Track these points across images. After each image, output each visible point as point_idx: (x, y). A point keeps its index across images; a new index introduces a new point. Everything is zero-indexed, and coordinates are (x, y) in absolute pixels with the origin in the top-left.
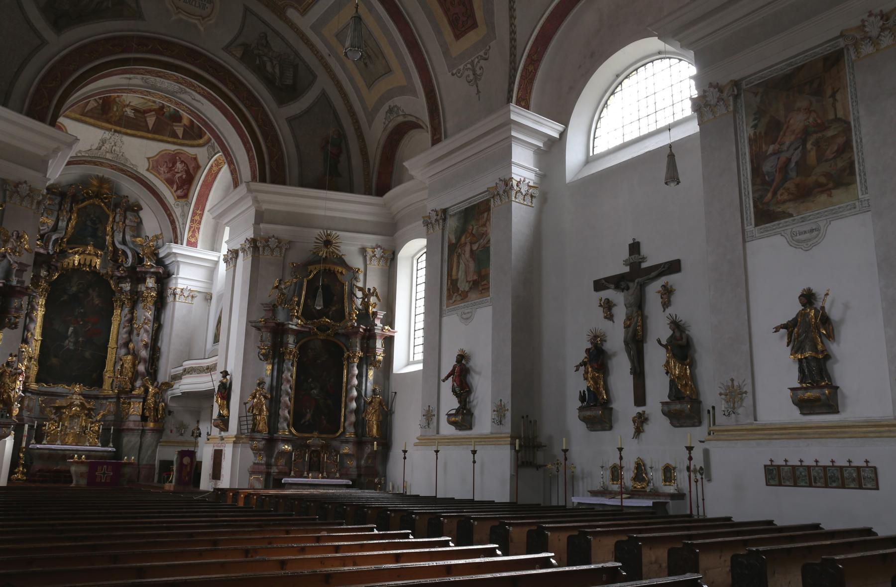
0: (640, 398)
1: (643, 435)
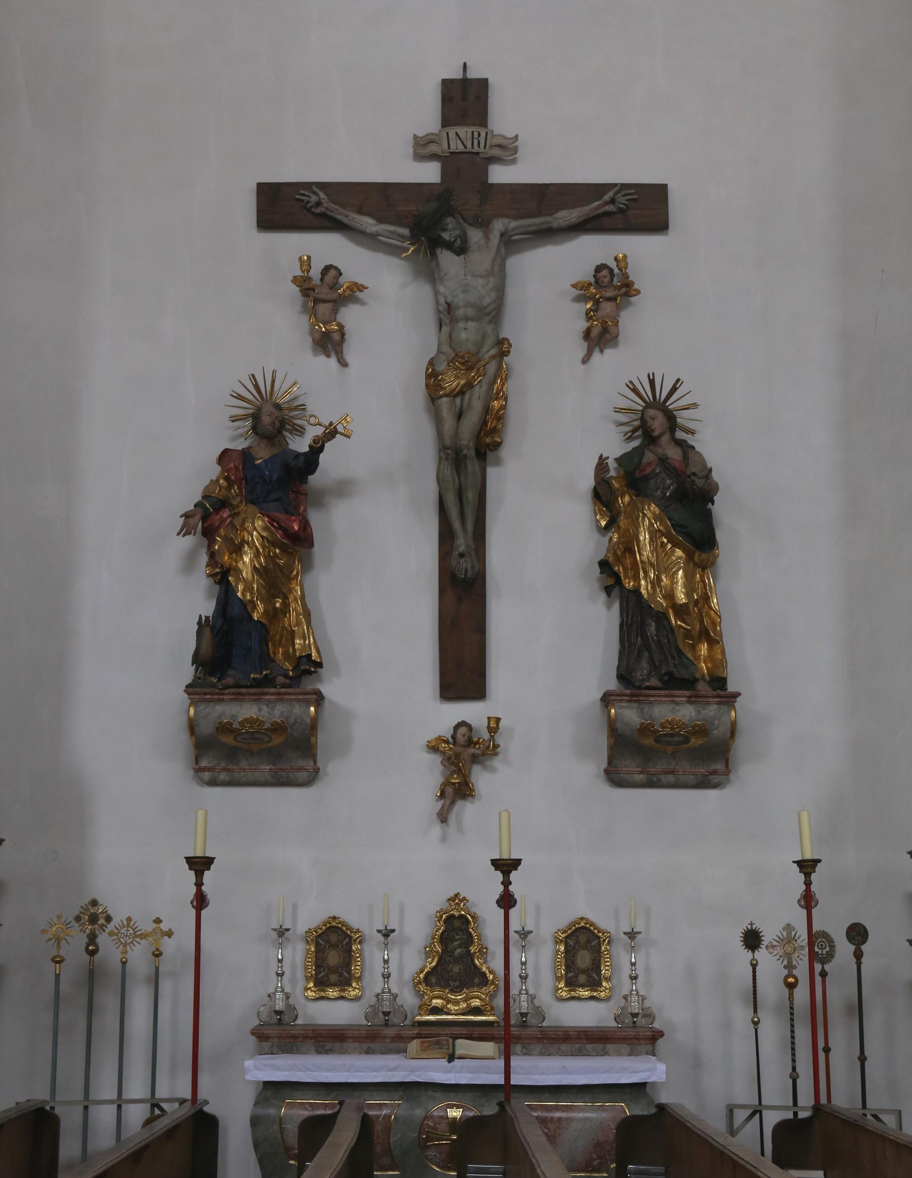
0: (463, 669)
1: (467, 810)
